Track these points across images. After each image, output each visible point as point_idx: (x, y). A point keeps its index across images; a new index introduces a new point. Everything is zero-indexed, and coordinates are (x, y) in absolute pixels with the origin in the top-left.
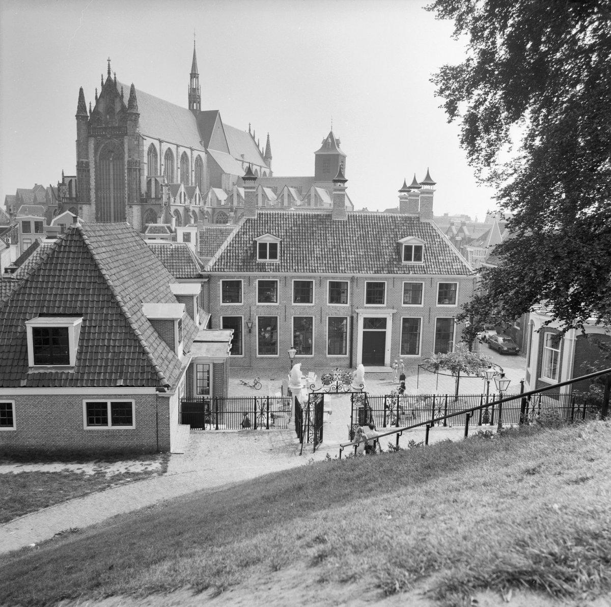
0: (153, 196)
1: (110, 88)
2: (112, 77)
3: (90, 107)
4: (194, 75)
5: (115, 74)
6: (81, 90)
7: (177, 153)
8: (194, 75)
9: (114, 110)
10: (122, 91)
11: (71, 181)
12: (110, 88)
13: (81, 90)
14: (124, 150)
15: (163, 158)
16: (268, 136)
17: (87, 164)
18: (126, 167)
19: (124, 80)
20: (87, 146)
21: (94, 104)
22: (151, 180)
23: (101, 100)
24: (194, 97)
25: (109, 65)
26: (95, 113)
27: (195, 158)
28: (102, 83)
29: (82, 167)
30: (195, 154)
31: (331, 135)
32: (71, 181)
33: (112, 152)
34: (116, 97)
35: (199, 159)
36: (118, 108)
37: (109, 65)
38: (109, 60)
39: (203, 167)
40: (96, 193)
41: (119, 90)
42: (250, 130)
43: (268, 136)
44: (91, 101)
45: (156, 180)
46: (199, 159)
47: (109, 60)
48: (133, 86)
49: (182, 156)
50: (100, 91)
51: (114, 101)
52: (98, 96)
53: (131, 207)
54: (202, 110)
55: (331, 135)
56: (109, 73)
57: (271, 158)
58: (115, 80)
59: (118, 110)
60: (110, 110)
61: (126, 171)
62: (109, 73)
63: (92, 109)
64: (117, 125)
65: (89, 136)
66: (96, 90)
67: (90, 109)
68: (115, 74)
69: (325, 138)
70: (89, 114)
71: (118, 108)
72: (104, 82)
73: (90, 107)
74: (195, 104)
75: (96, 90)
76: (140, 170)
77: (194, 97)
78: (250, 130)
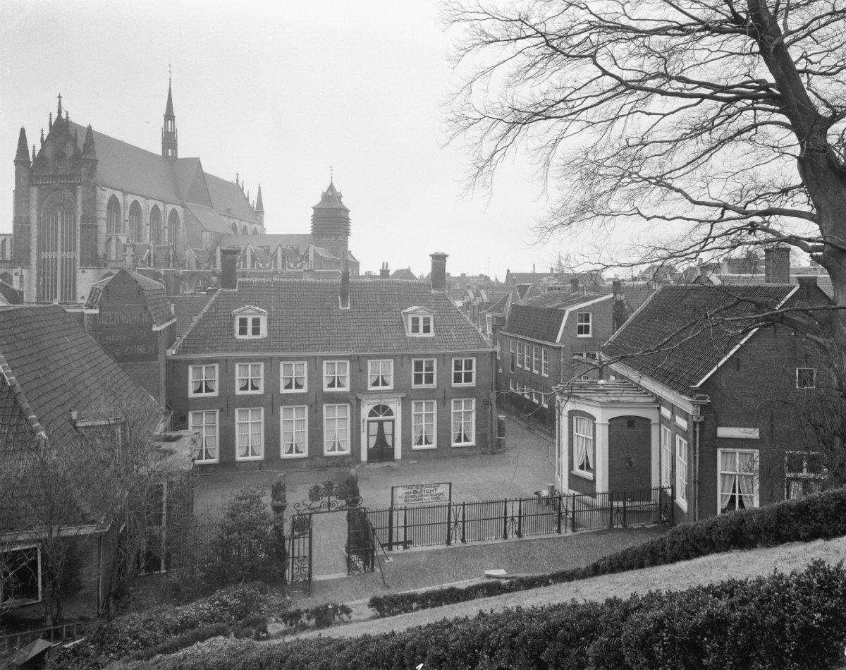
0: (113, 258)
1: (61, 128)
2: (64, 116)
3: (34, 151)
4: (169, 116)
5: (67, 113)
6: (23, 131)
7: (146, 206)
8: (169, 116)
10: (76, 134)
11: (5, 239)
12: (61, 128)
13: (23, 131)
15: (128, 213)
16: (260, 187)
17: (28, 220)
18: (79, 223)
19: (79, 118)
20: (28, 196)
21: (38, 148)
22: (111, 238)
24: (169, 140)
25: (60, 103)
26: (40, 158)
27: (168, 213)
29: (21, 223)
30: (170, 207)
31: (331, 187)
32: (5, 239)
35: (174, 212)
36: (70, 152)
37: (60, 103)
39: (179, 223)
40: (39, 254)
41: (72, 132)
42: (237, 180)
43: (260, 187)
44: (34, 144)
45: (117, 239)
46: (174, 212)
47: (60, 97)
48: (90, 127)
49: (153, 209)
50: (47, 132)
51: (65, 144)
52: (45, 137)
53: (83, 272)
54: (180, 156)
55: (331, 187)
56: (60, 112)
57: (263, 212)
58: (67, 117)
59: (70, 155)
60: (60, 155)
61: (79, 228)
62: (60, 112)
63: (37, 153)
65: (33, 185)
66: (42, 131)
68: (67, 113)
69: (325, 191)
70: (31, 160)
71: (70, 152)
72: (53, 121)
73: (34, 151)
74: (170, 150)
75: (42, 131)
76: (96, 227)
77: (169, 140)
78: (237, 180)
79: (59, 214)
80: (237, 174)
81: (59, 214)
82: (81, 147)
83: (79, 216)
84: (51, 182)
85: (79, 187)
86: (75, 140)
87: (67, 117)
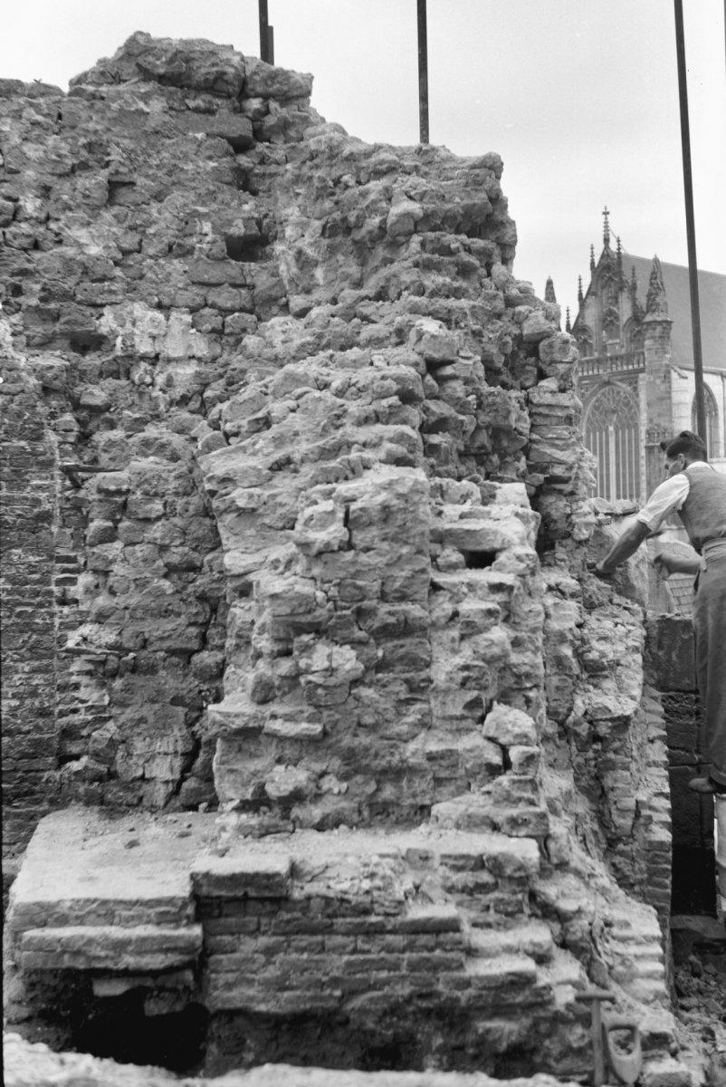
2: (613, 246)
3: (568, 318)
5: (618, 241)
6: (550, 283)
9: (617, 318)
13: (550, 283)
14: (638, 406)
18: (643, 444)
21: (575, 311)
23: (589, 301)
25: (606, 223)
28: (593, 263)
33: (614, 412)
34: (621, 289)
37: (606, 223)
38: (606, 213)
47: (606, 213)
56: (606, 240)
60: (609, 321)
61: (643, 453)
62: (606, 240)
64: (623, 351)
67: (568, 325)
68: (618, 241)
73: (568, 318)
79: (611, 428)
80: (592, 248)
81: (611, 428)
82: (642, 300)
83: (643, 429)
84: (596, 372)
85: (641, 376)
86: (634, 288)
87: (619, 249)
